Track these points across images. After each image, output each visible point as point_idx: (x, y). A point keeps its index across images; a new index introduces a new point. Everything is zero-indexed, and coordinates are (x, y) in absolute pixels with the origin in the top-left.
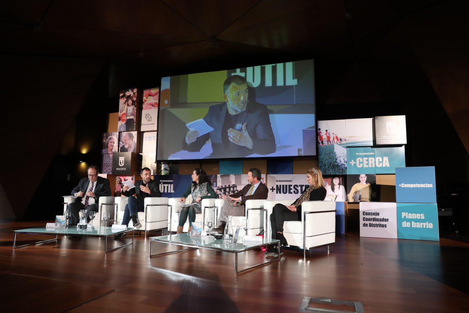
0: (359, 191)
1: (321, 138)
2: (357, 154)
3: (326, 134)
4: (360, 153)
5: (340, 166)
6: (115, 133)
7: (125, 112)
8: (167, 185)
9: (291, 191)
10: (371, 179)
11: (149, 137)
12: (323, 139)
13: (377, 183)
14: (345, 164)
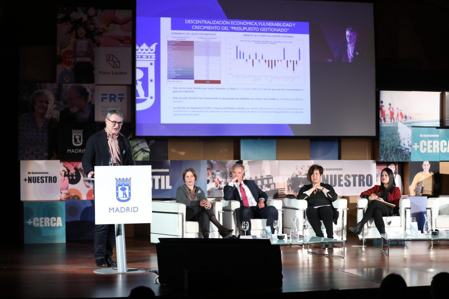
0: (421, 182)
1: (383, 113)
2: (421, 136)
3: (389, 109)
4: (424, 135)
5: (403, 151)
6: (49, 85)
7: (70, 48)
8: (159, 177)
9: (342, 183)
10: (434, 166)
11: (111, 95)
12: (386, 115)
13: (441, 173)
14: (409, 148)
